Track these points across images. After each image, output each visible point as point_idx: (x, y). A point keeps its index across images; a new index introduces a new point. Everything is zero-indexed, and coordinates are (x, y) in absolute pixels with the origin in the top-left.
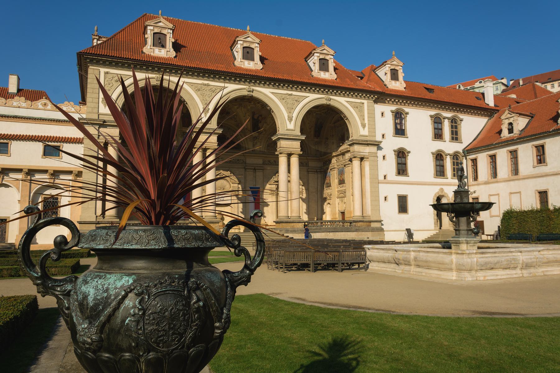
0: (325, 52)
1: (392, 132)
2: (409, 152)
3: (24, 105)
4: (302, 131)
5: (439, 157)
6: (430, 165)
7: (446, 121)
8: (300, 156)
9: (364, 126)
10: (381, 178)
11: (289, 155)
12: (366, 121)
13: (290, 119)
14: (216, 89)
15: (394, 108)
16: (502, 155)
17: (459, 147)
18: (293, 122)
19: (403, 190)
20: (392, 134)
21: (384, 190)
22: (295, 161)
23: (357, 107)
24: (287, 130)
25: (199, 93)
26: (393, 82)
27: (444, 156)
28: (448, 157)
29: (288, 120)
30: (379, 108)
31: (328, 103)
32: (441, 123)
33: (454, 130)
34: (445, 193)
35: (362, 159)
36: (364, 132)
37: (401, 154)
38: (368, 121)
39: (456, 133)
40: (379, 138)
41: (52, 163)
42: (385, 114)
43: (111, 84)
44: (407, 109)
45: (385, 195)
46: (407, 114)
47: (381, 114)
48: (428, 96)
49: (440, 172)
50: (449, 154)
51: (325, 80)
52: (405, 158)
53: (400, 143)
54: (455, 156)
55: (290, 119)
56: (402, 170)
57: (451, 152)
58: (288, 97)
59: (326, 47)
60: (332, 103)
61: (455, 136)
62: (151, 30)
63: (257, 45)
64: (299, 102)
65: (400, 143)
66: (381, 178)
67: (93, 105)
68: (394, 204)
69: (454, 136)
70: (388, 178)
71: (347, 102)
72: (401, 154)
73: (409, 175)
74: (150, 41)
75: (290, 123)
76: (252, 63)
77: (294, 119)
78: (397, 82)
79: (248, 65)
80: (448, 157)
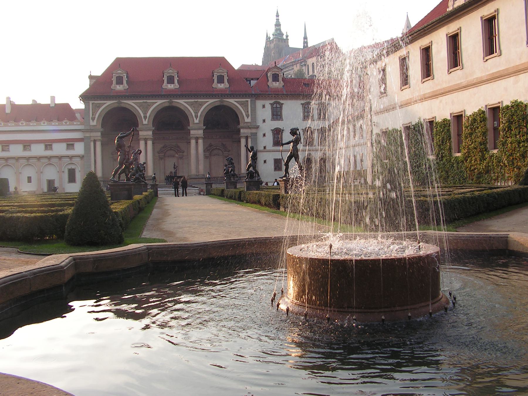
0: (220, 71)
3: (57, 124)
8: (204, 138)
11: (197, 139)
13: (197, 117)
15: (272, 102)
20: (271, 119)
23: (243, 104)
26: (274, 83)
30: (259, 103)
31: (222, 104)
35: (247, 138)
36: (248, 120)
42: (266, 106)
44: (282, 102)
45: (265, 159)
46: (283, 104)
55: (197, 117)
62: (115, 76)
66: (262, 148)
68: (271, 165)
70: (267, 148)
71: (235, 101)
74: (114, 82)
75: (196, 119)
76: (172, 85)
77: (199, 116)
78: (278, 83)
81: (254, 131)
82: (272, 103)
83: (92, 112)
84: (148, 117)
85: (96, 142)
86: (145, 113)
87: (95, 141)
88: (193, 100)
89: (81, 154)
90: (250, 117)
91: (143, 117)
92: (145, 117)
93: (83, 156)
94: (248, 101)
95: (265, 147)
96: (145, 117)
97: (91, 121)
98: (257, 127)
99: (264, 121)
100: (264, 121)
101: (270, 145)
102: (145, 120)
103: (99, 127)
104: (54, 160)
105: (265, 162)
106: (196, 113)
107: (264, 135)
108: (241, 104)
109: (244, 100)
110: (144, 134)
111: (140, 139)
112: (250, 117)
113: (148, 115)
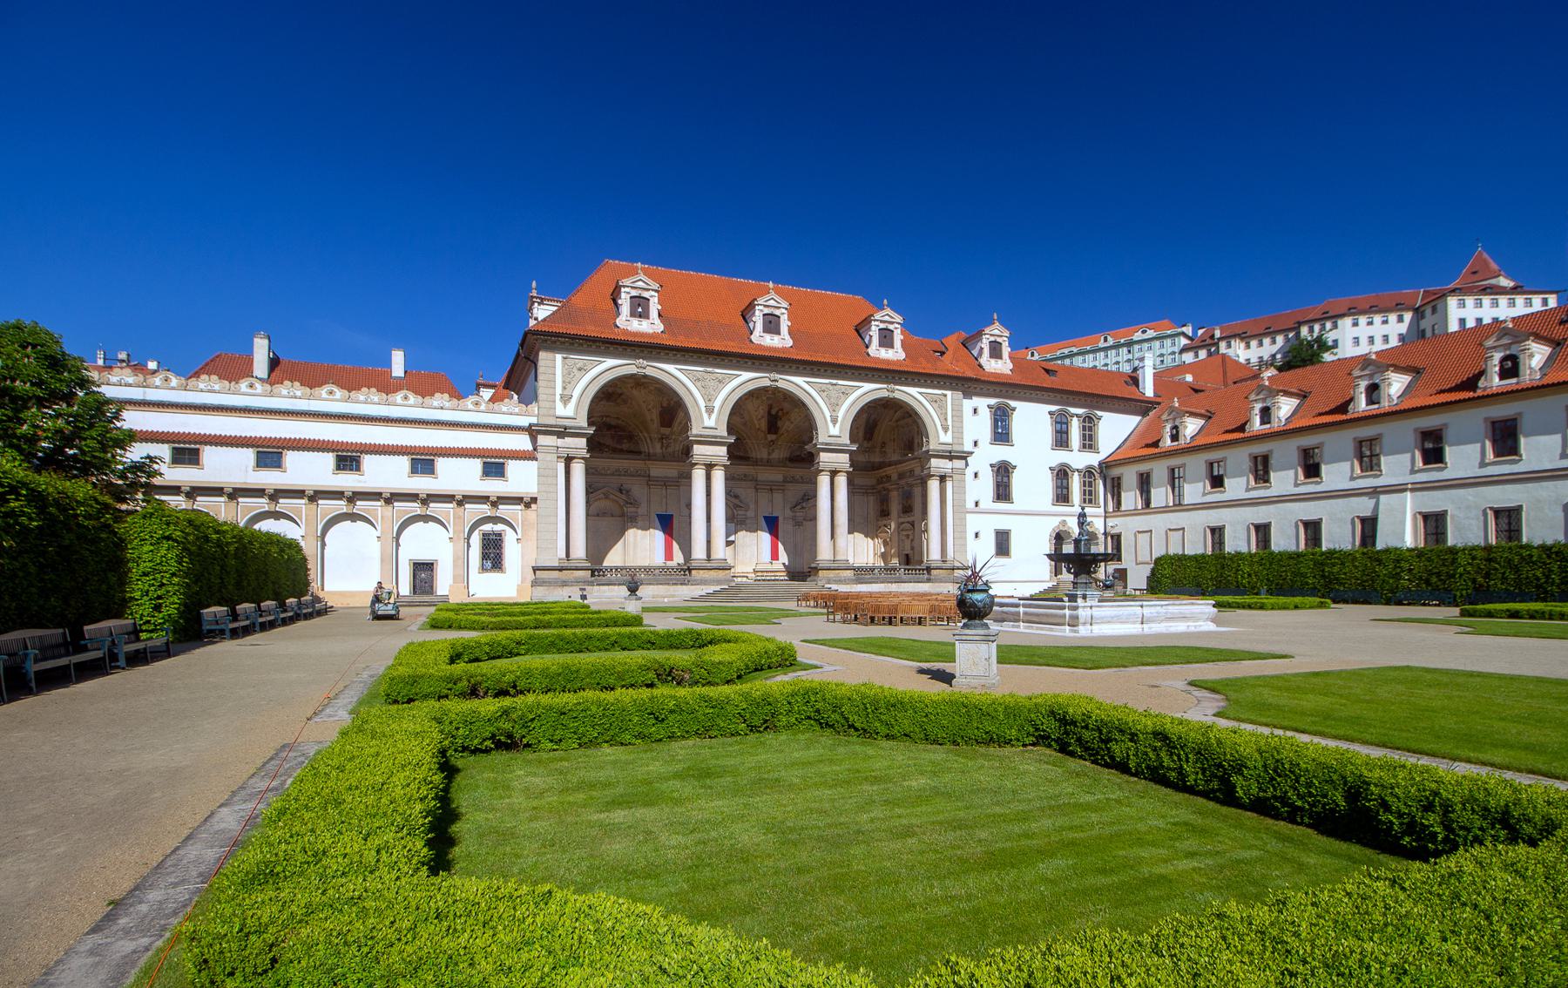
1: (990, 436)
2: (1015, 467)
4: (853, 439)
5: (1062, 474)
6: (1047, 486)
7: (1075, 419)
9: (946, 429)
10: (970, 505)
11: (834, 473)
12: (950, 422)
13: (834, 421)
14: (724, 379)
15: (993, 401)
16: (1159, 470)
17: (1093, 459)
18: (838, 425)
19: (1003, 523)
20: (989, 440)
21: (973, 522)
22: (842, 481)
23: (936, 401)
24: (830, 436)
25: (699, 384)
26: (993, 361)
27: (1070, 473)
28: (1076, 473)
29: (832, 421)
30: (968, 404)
31: (892, 395)
32: (1067, 424)
33: (1087, 433)
34: (1069, 528)
35: (943, 479)
36: (946, 438)
37: (1003, 472)
38: (953, 421)
39: (1091, 438)
40: (968, 447)
41: (494, 487)
42: (979, 411)
43: (573, 374)
44: (1013, 403)
47: (972, 411)
48: (1048, 381)
49: (1062, 497)
50: (1077, 470)
51: (888, 362)
52: (1008, 477)
53: (1001, 453)
54: (1088, 472)
55: (834, 421)
56: (1003, 492)
57: (1080, 466)
58: (831, 387)
59: (888, 311)
60: (897, 395)
61: (1089, 443)
63: (784, 311)
64: (846, 394)
65: (1001, 453)
67: (547, 405)
69: (1087, 442)
70: (982, 505)
72: (1003, 472)
73: (1014, 501)
76: (776, 338)
77: (839, 419)
78: (1000, 362)
79: (771, 341)
80: (1076, 473)
81: (959, 464)
82: (992, 403)
83: (564, 382)
84: (716, 410)
85: (569, 465)
86: (709, 399)
87: (569, 460)
88: (827, 381)
89: (527, 493)
90: (950, 433)
91: (703, 409)
92: (710, 410)
93: (531, 498)
94: (945, 396)
95: (977, 504)
96: (710, 410)
97: (559, 405)
98: (964, 456)
99: (976, 443)
100: (976, 443)
101: (987, 500)
102: (710, 418)
103: (582, 422)
104: (435, 508)
105: (977, 535)
106: (834, 411)
107: (976, 475)
108: (933, 401)
109: (939, 392)
110: (708, 453)
111: (696, 464)
112: (950, 433)
113: (717, 404)
